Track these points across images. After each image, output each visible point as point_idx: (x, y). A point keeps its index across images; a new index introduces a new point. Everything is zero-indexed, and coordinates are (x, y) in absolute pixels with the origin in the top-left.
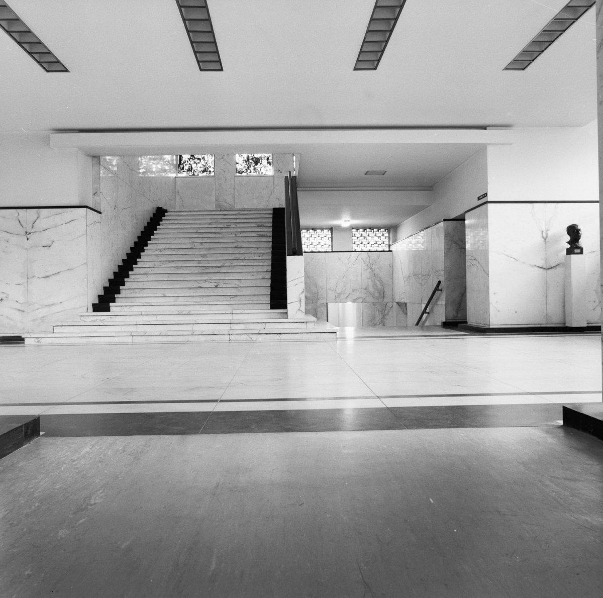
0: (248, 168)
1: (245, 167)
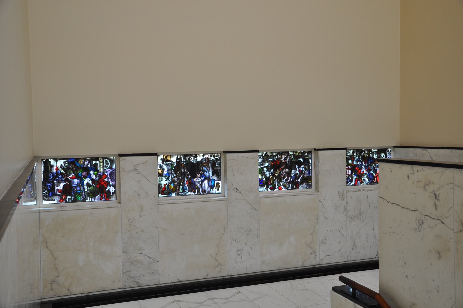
0: (179, 184)
1: (174, 181)
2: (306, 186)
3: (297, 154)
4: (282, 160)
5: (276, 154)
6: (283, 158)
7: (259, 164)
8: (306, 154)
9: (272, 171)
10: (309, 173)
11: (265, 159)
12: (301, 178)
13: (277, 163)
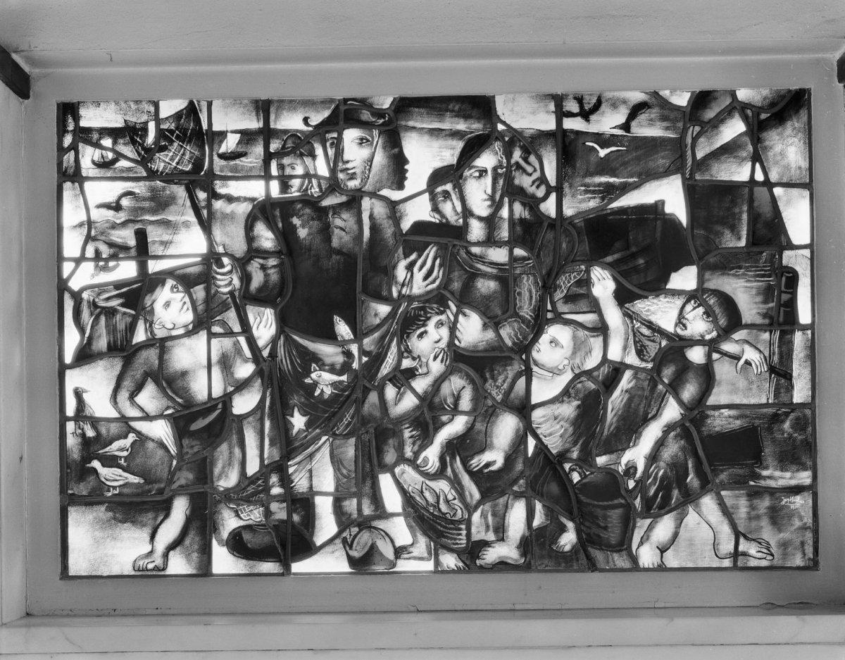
2: (738, 535)
3: (608, 122)
4: (395, 195)
5: (317, 118)
6: (417, 177)
7: (89, 238)
8: (735, 128)
9: (264, 325)
10: (780, 372)
11: (171, 177)
12: (669, 428)
13: (326, 231)
